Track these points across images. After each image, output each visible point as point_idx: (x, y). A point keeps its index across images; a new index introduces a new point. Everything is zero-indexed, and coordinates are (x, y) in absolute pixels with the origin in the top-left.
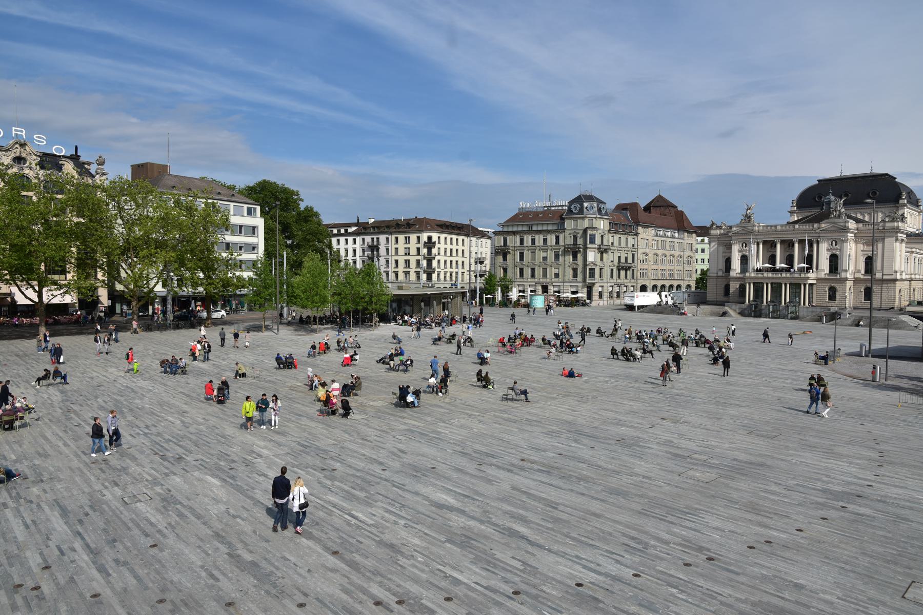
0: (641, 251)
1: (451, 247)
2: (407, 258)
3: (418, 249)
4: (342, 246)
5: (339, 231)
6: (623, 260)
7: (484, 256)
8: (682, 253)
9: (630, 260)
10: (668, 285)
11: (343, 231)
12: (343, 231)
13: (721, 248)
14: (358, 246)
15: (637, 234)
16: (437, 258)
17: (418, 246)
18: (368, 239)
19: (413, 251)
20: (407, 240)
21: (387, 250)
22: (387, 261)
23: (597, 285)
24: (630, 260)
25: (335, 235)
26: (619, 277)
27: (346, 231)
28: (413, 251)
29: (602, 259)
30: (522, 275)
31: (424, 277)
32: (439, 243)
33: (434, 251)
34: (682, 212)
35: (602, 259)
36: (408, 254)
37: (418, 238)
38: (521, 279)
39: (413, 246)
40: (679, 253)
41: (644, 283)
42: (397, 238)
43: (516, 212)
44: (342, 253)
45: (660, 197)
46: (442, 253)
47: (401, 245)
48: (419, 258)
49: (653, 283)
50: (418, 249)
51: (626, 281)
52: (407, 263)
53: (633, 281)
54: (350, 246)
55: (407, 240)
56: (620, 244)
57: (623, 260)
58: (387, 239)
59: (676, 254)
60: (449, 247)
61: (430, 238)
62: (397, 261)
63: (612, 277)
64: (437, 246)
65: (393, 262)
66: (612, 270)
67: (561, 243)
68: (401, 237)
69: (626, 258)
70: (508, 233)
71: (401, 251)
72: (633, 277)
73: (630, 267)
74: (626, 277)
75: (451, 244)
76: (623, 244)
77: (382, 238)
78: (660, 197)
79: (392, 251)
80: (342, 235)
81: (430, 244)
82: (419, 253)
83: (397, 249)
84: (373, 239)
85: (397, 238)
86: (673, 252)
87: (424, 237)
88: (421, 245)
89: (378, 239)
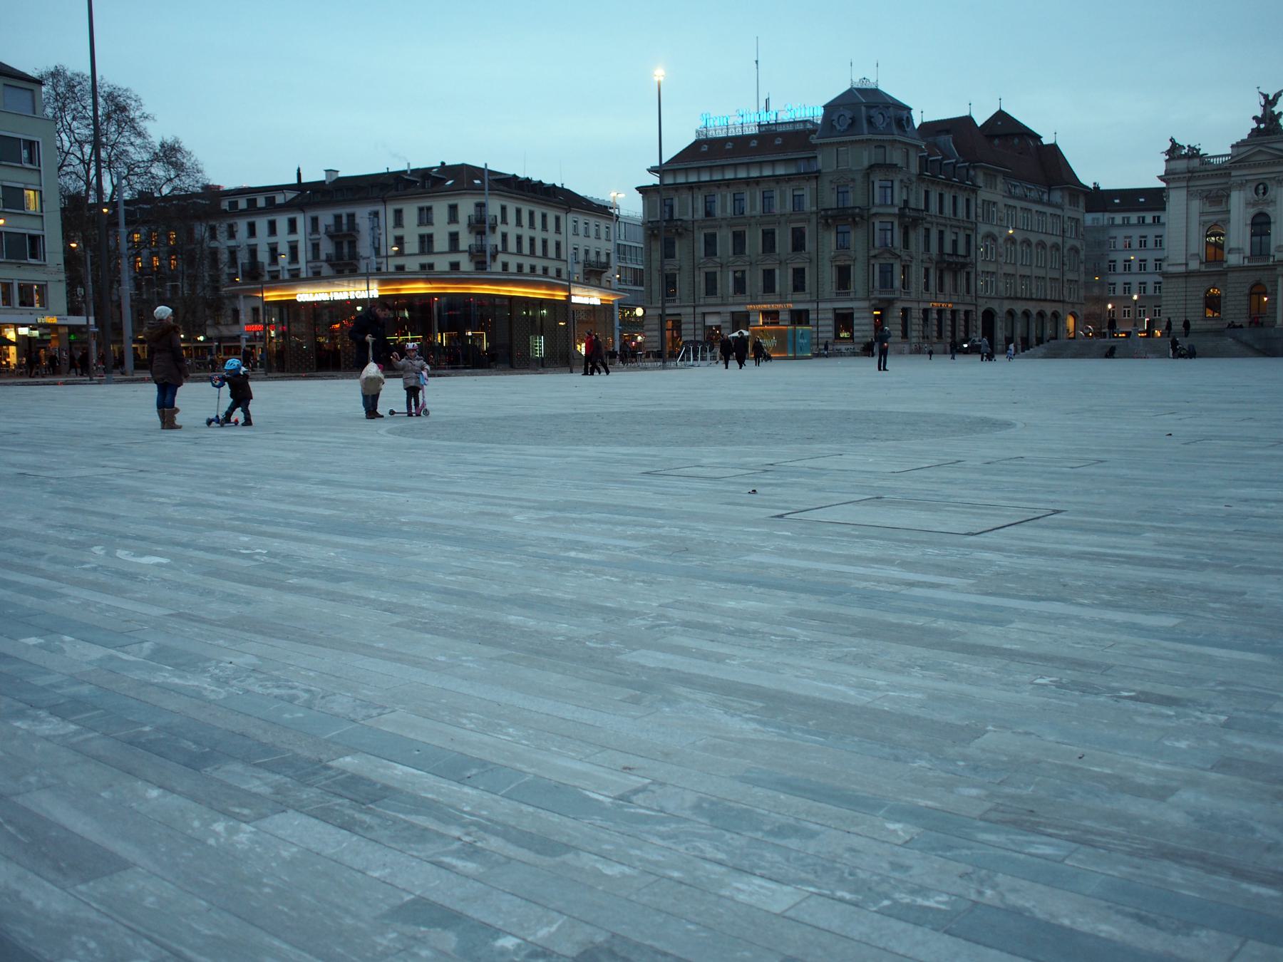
0: (983, 229)
1: (532, 233)
2: (426, 259)
3: (454, 237)
4: (262, 240)
6: (948, 248)
7: (603, 259)
8: (1059, 240)
9: (961, 251)
10: (1034, 312)
11: (261, 202)
12: (261, 202)
13: (1196, 205)
14: (301, 236)
15: (974, 189)
16: (501, 258)
17: (454, 228)
18: (326, 218)
19: (441, 243)
20: (425, 216)
23: (900, 305)
24: (961, 251)
25: (243, 213)
26: (941, 290)
27: (271, 201)
28: (441, 243)
29: (906, 244)
30: (711, 288)
32: (504, 221)
33: (494, 240)
34: (1054, 148)
35: (906, 244)
38: (711, 300)
39: (440, 230)
40: (1054, 239)
41: (989, 305)
43: (691, 139)
44: (264, 257)
45: (1001, 116)
46: (512, 246)
48: (454, 258)
49: (1007, 305)
50: (454, 237)
51: (955, 299)
53: (968, 299)
54: (283, 238)
55: (425, 216)
56: (941, 211)
57: (948, 248)
59: (1049, 240)
60: (526, 233)
61: (480, 206)
63: (927, 288)
64: (501, 228)
66: (927, 270)
67: (808, 206)
68: (411, 212)
69: (955, 243)
70: (676, 187)
71: (412, 245)
72: (968, 291)
73: (964, 265)
74: (955, 290)
75: (532, 225)
76: (948, 210)
77: (362, 214)
78: (1001, 116)
80: (261, 212)
83: (399, 241)
84: (338, 218)
85: (398, 213)
86: (1043, 237)
87: (466, 207)
88: (461, 227)
89: (351, 217)
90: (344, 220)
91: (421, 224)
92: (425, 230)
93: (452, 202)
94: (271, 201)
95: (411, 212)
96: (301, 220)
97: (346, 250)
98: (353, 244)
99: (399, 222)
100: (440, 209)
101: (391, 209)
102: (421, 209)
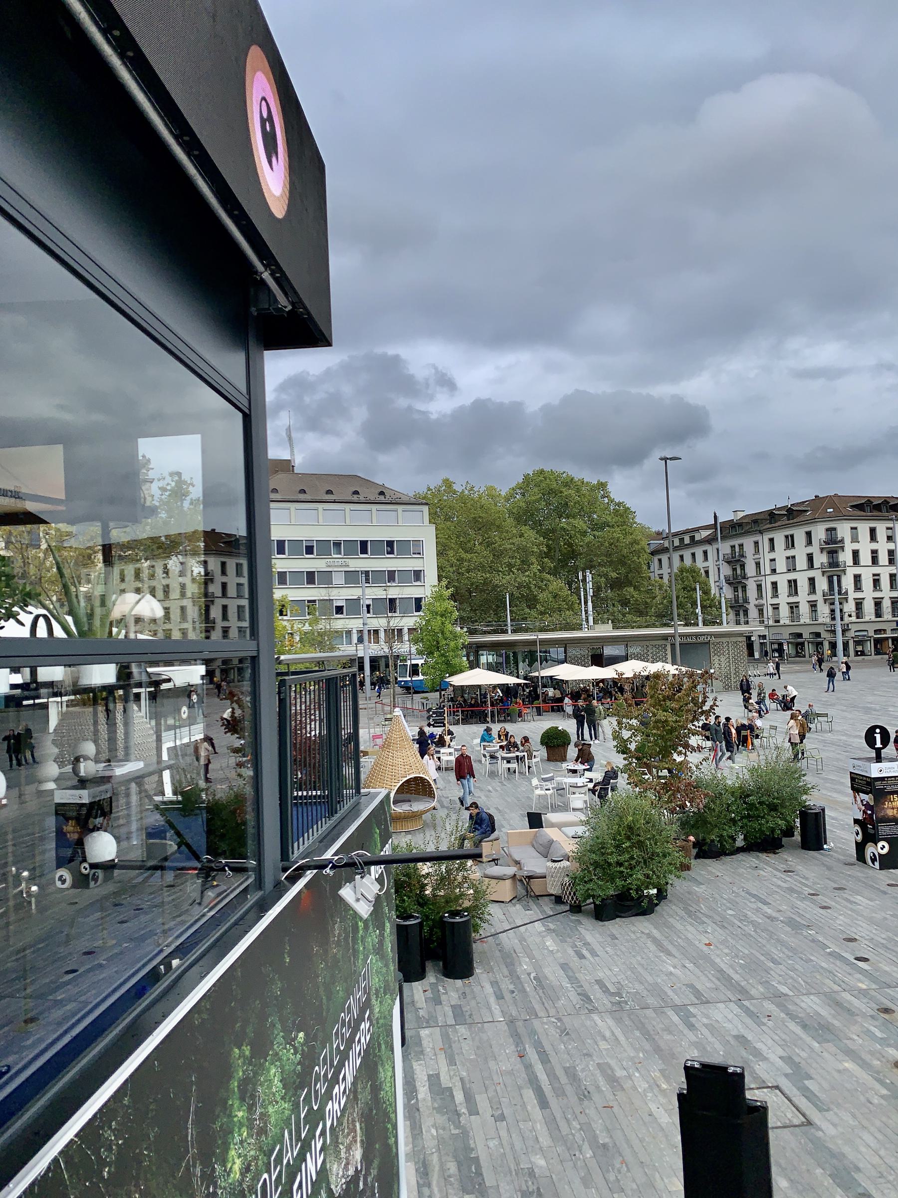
2: (792, 576)
3: (810, 558)
5: (682, 540)
11: (687, 540)
17: (809, 550)
18: (725, 548)
20: (790, 542)
21: (758, 564)
22: (759, 587)
25: (676, 549)
28: (802, 563)
31: (824, 610)
36: (792, 569)
37: (809, 534)
39: (800, 552)
42: (772, 540)
47: (781, 554)
48: (811, 574)
50: (810, 558)
52: (793, 585)
55: (790, 542)
58: (756, 543)
65: (769, 586)
68: (780, 538)
71: (781, 566)
77: (748, 543)
79: (766, 568)
81: (833, 546)
82: (811, 566)
84: (733, 547)
87: (819, 532)
88: (815, 549)
89: (741, 546)
90: (737, 549)
91: (787, 548)
92: (790, 553)
93: (808, 529)
95: (780, 538)
97: (739, 572)
98: (743, 566)
100: (799, 535)
101: (767, 537)
102: (787, 537)
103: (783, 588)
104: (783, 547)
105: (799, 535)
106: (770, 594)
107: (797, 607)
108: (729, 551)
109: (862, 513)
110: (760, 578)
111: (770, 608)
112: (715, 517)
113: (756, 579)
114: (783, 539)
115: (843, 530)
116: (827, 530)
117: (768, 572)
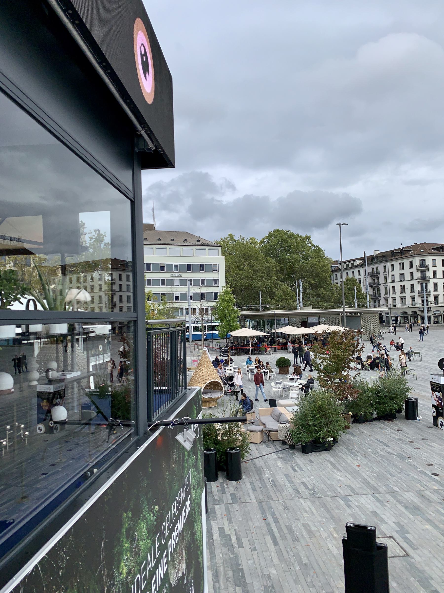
2: (402, 283)
3: (412, 274)
5: (347, 265)
11: (350, 265)
17: (411, 270)
18: (369, 269)
20: (402, 266)
21: (385, 277)
22: (386, 288)
25: (345, 269)
27: (353, 264)
31: (418, 300)
36: (403, 280)
37: (411, 263)
39: (407, 271)
42: (392, 266)
47: (397, 272)
48: (412, 282)
50: (412, 274)
52: (403, 288)
55: (402, 266)
58: (385, 267)
62: (394, 287)
65: (391, 288)
68: (396, 264)
71: (397, 278)
77: (381, 267)
81: (423, 268)
82: (412, 278)
84: (373, 269)
87: (417, 262)
88: (414, 270)
89: (377, 268)
90: (375, 270)
91: (400, 269)
92: (402, 272)
93: (411, 260)
94: (353, 264)
95: (396, 264)
96: (362, 270)
97: (376, 281)
98: (378, 278)
99: (393, 270)
100: (406, 263)
101: (390, 264)
102: (400, 264)
103: (398, 289)
104: (398, 268)
105: (406, 263)
106: (391, 292)
107: (405, 299)
108: (371, 270)
109: (439, 252)
110: (386, 284)
111: (391, 300)
112: (364, 254)
113: (384, 285)
114: (398, 265)
115: (429, 260)
116: (421, 260)
117: (391, 281)
